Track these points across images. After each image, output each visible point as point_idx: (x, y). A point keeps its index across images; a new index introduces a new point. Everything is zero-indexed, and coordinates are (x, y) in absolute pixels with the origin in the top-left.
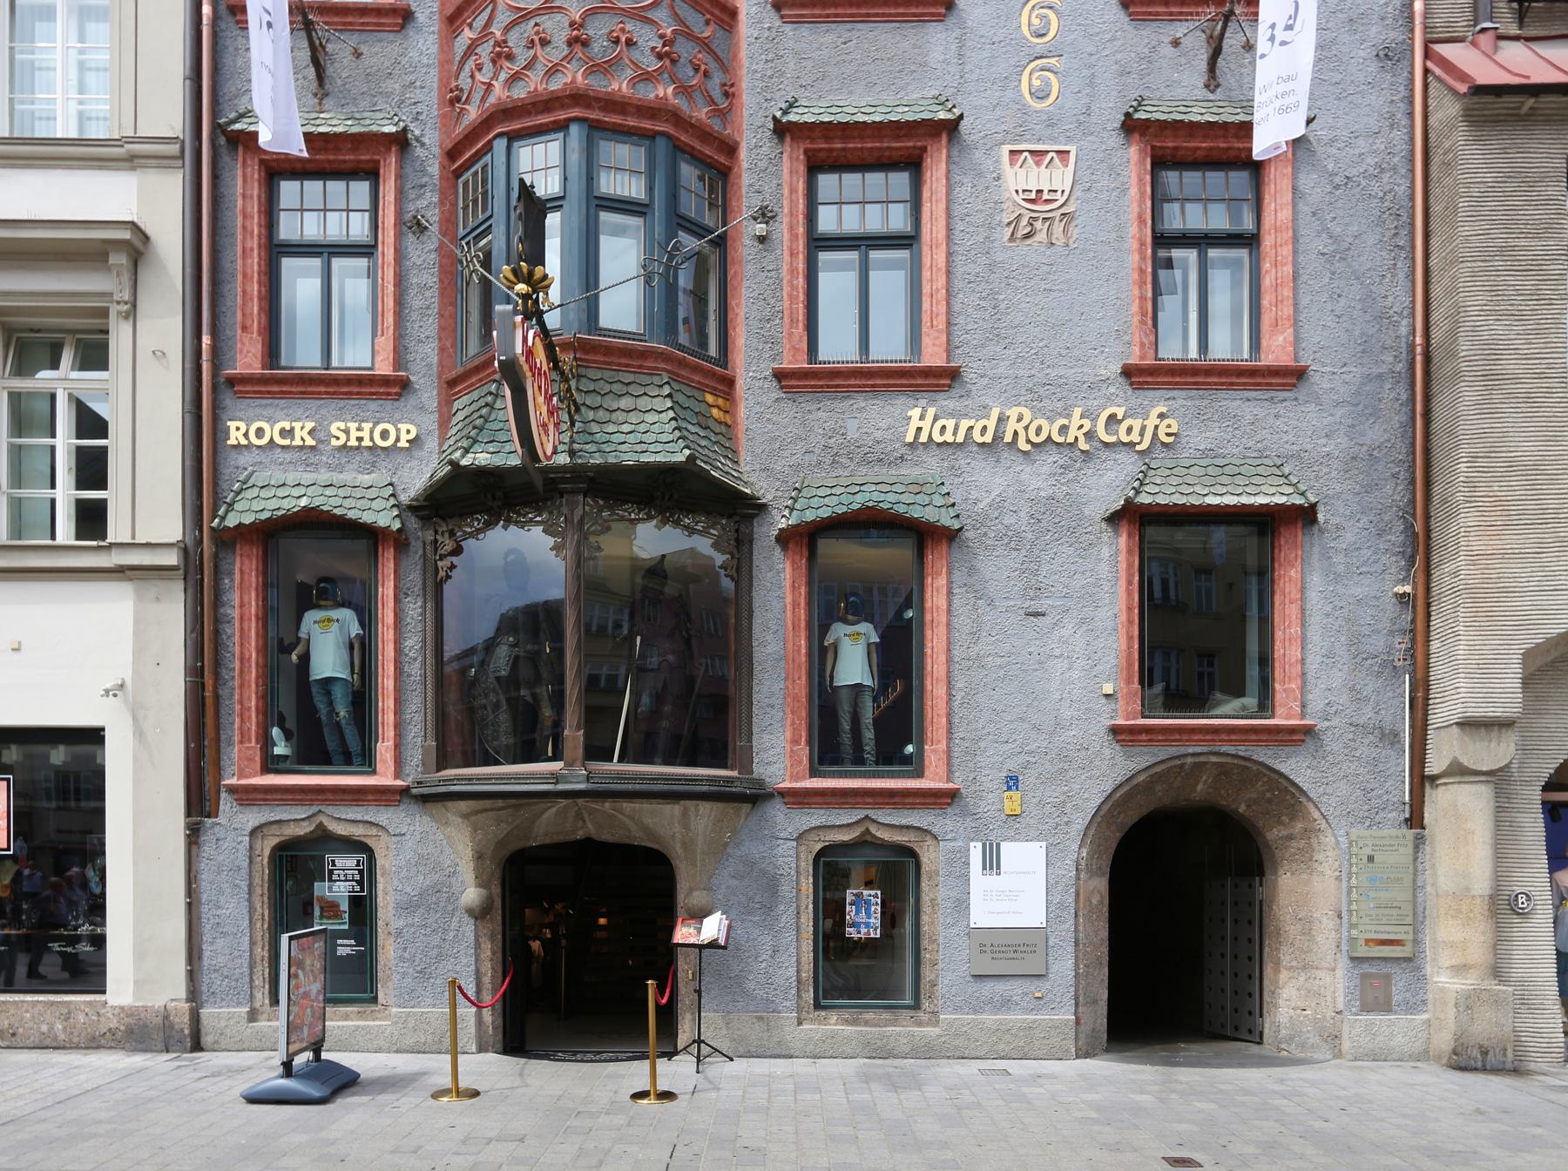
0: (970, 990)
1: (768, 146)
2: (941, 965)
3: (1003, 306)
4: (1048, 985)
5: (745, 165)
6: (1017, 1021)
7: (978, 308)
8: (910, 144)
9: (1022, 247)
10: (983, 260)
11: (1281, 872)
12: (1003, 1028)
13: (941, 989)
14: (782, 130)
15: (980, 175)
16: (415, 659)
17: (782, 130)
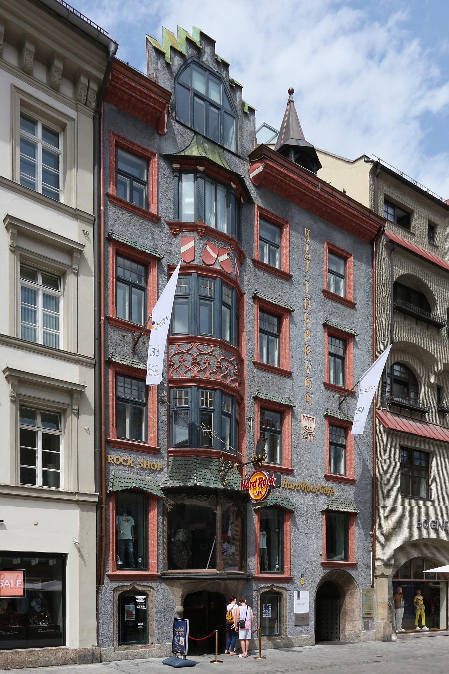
0: (294, 629)
1: (252, 401)
2: (288, 623)
3: (301, 455)
4: (309, 627)
5: (246, 405)
6: (304, 636)
7: (297, 455)
8: (283, 409)
9: (305, 441)
10: (297, 442)
11: (346, 597)
12: (301, 638)
13: (288, 629)
14: (256, 399)
15: (297, 420)
16: (161, 536)
17: (256, 399)
